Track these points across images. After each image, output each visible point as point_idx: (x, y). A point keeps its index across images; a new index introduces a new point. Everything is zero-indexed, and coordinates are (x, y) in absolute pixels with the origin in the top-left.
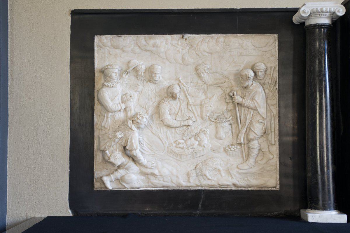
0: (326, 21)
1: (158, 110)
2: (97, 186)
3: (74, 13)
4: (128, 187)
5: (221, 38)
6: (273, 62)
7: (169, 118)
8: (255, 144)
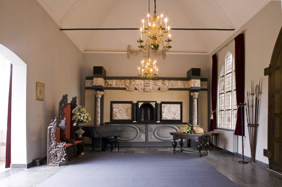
0: (135, 103)
1: (119, 111)
2: (113, 119)
3: (111, 101)
4: (116, 119)
5: (126, 104)
6: (131, 107)
7: (120, 112)
8: (129, 115)
